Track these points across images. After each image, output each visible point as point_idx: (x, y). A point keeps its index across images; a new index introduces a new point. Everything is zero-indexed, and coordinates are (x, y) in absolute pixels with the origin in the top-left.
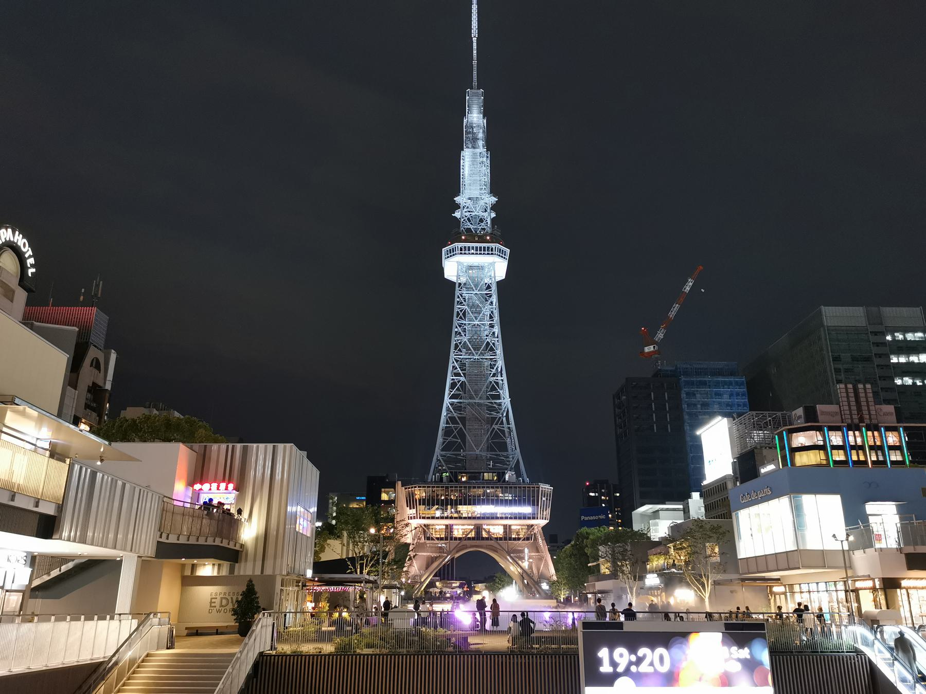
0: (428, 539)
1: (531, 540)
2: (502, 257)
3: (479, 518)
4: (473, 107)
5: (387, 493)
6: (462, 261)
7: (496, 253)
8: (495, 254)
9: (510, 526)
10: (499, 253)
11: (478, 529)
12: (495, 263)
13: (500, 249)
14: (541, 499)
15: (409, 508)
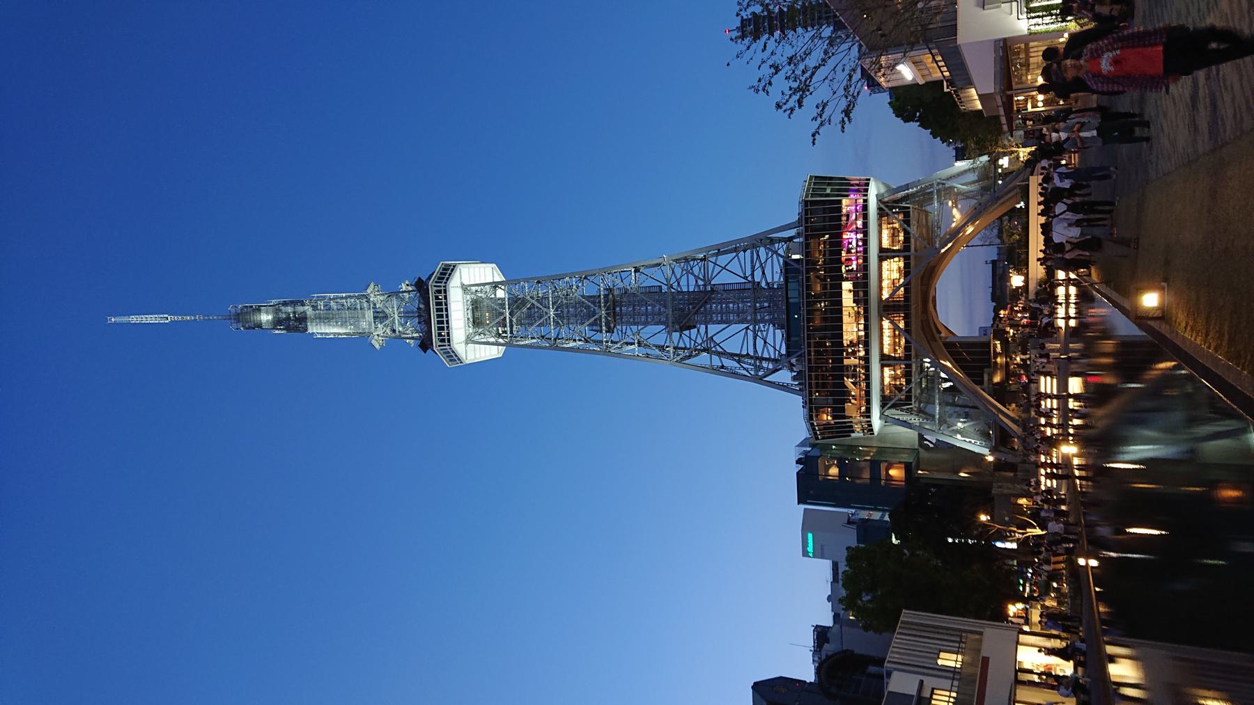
0: (909, 398)
1: (909, 208)
2: (450, 274)
3: (866, 310)
4: (254, 321)
5: (829, 467)
6: (463, 338)
7: (443, 284)
8: (445, 286)
9: (882, 250)
10: (444, 281)
11: (888, 308)
12: (463, 285)
13: (439, 278)
14: (827, 195)
15: (853, 435)
